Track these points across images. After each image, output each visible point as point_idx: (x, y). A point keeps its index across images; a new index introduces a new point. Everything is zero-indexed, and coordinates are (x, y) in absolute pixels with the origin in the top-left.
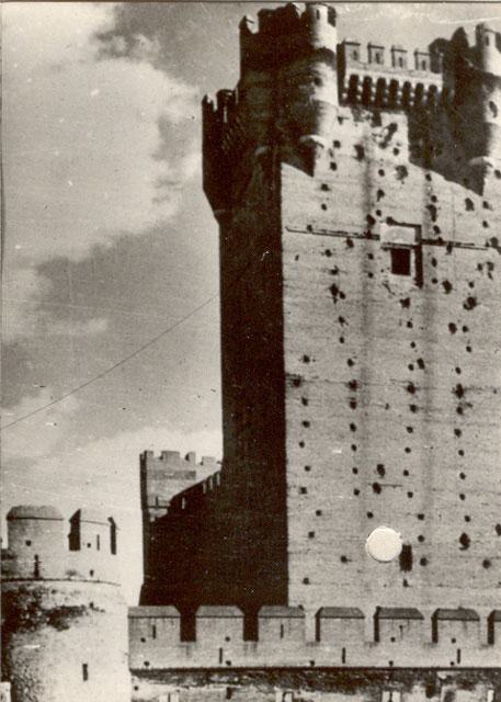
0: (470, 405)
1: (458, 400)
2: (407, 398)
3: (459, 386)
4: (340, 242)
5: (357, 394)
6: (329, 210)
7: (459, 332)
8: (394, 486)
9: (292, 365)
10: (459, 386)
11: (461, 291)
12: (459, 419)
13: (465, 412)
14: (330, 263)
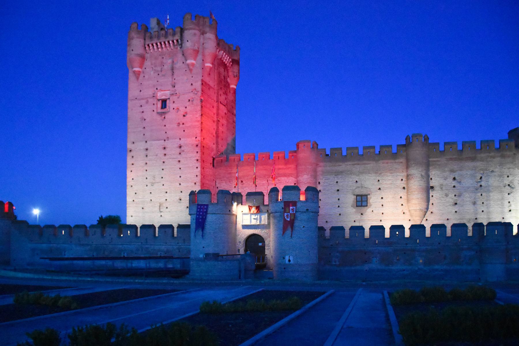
0: (183, 151)
1: (179, 150)
2: (164, 152)
3: (180, 145)
4: (143, 102)
5: (148, 152)
6: (142, 92)
7: (181, 126)
8: (158, 183)
9: (129, 146)
10: (180, 145)
11: (182, 110)
12: (179, 156)
13: (181, 153)
14: (141, 109)
